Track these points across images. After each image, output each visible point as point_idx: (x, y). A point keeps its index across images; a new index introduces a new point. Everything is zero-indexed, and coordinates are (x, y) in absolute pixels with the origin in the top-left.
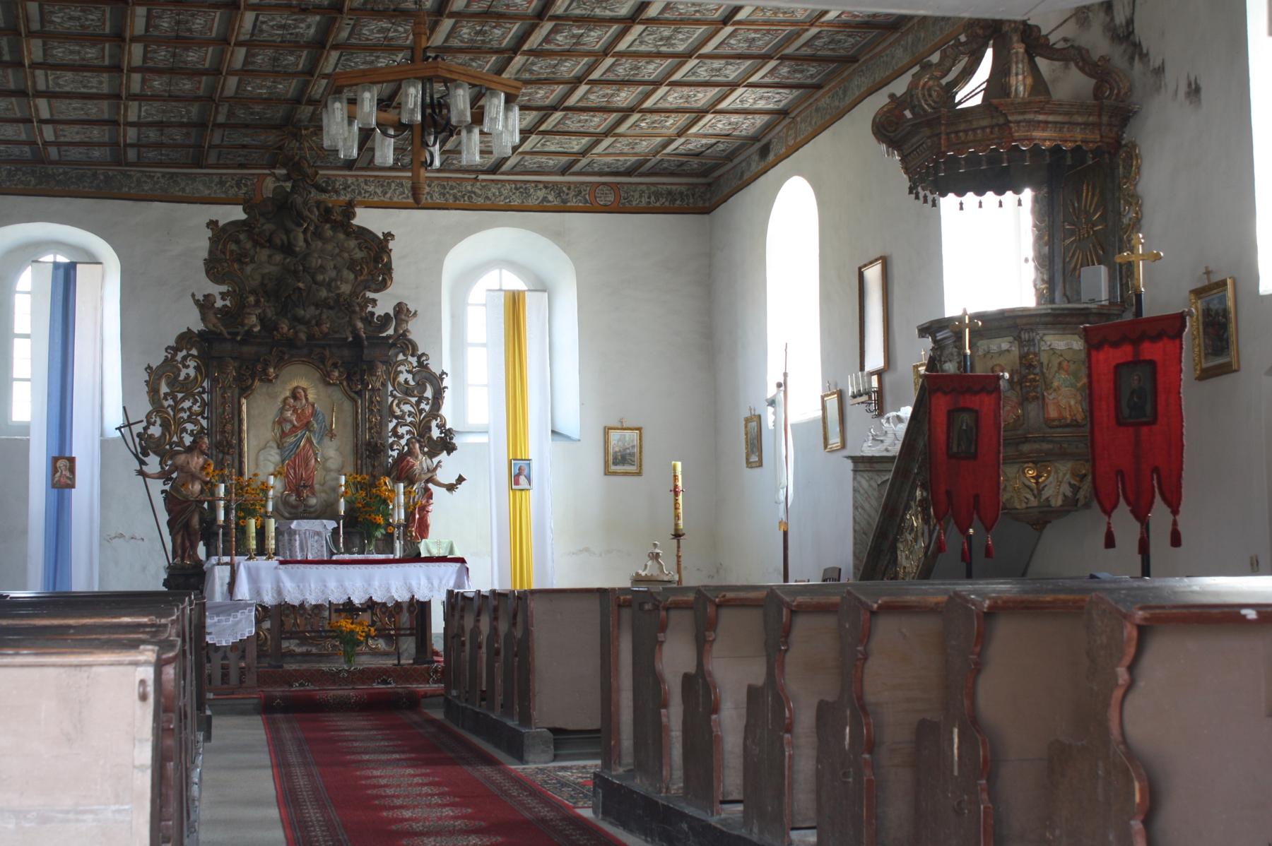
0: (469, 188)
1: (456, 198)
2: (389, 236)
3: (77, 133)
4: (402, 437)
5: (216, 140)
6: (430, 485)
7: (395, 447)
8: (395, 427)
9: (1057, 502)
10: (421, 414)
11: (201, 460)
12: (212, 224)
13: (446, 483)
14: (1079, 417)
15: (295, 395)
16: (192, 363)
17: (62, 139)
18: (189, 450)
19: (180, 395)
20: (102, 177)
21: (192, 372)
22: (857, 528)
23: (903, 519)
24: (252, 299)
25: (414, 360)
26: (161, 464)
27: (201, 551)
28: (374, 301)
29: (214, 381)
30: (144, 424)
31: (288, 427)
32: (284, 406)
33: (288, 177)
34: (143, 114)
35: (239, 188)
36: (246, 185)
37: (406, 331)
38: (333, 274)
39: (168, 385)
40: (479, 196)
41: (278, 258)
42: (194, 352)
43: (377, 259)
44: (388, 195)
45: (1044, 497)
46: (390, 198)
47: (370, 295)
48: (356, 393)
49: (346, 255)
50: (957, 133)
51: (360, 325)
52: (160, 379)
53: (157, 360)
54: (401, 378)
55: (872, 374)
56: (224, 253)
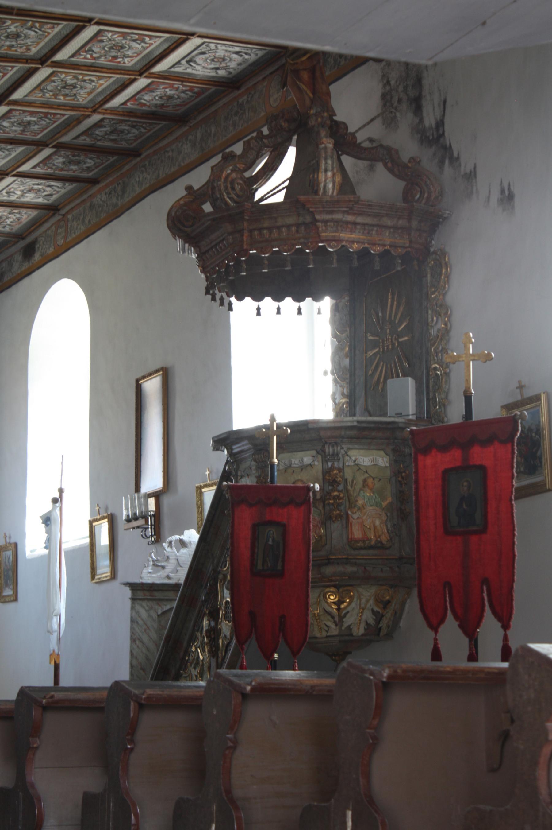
9: (359, 631)
14: (384, 539)
22: (135, 662)
23: (187, 652)
45: (345, 625)
50: (260, 230)
55: (149, 495)
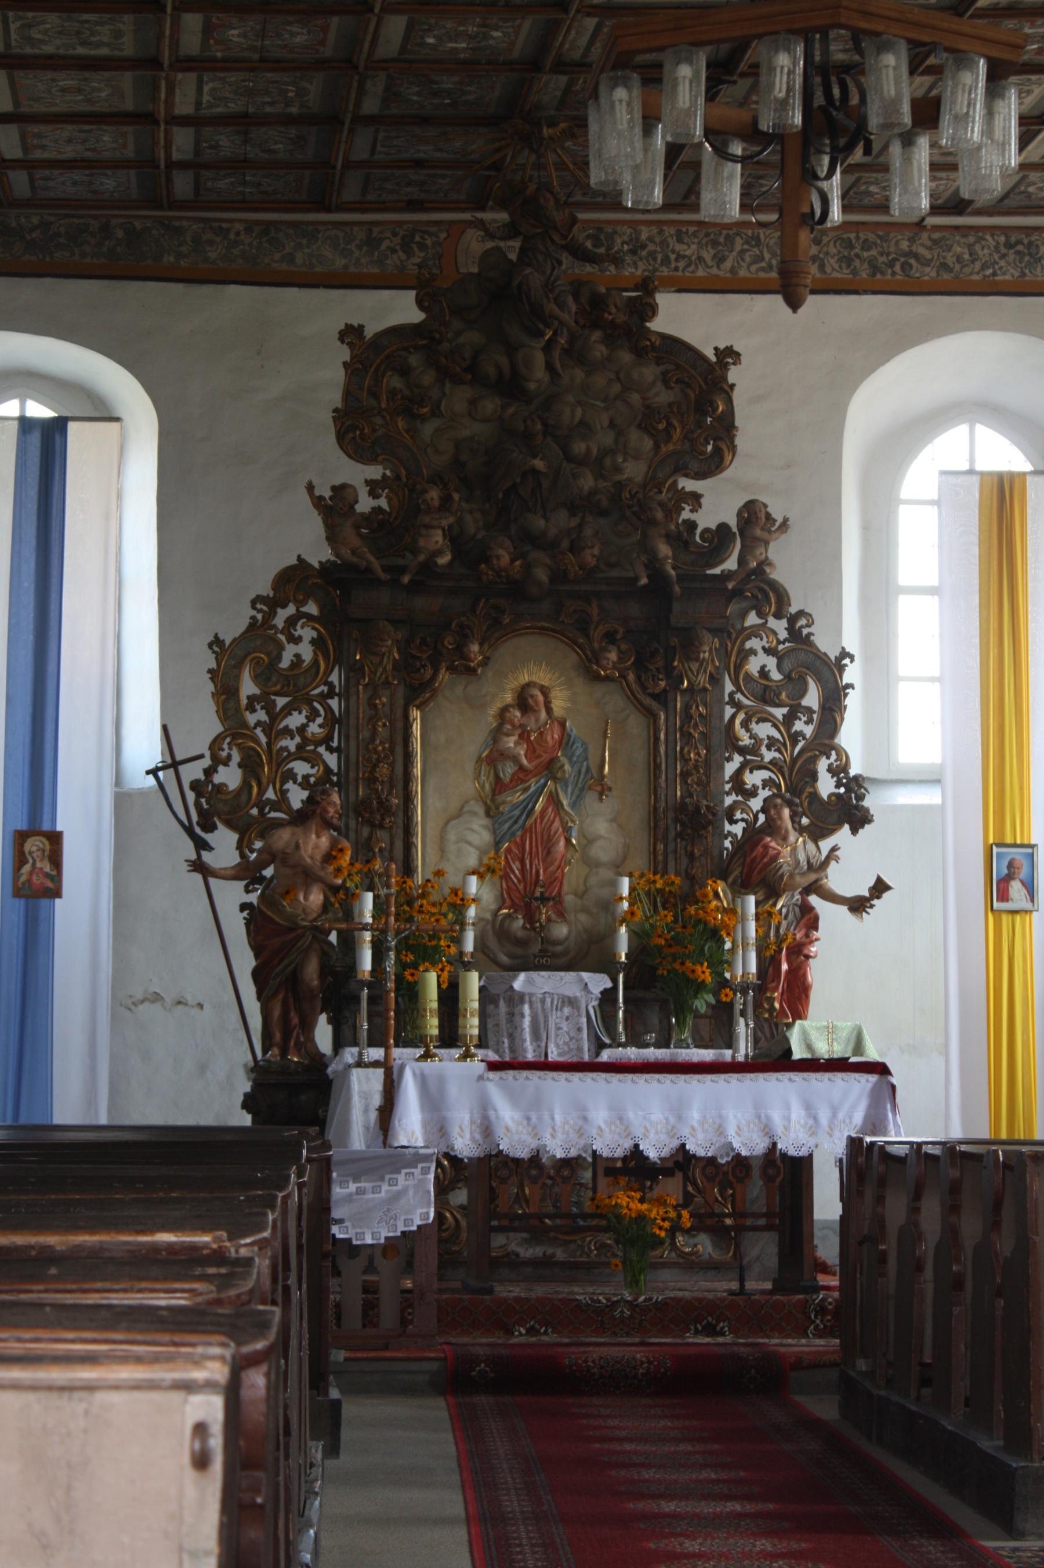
0: (904, 245)
1: (875, 269)
2: (728, 355)
3: (69, 141)
4: (753, 793)
5: (360, 150)
6: (814, 900)
7: (738, 815)
8: (739, 772)
10: (794, 743)
11: (324, 841)
12: (351, 334)
13: (849, 893)
15: (523, 702)
16: (307, 633)
17: (38, 154)
18: (301, 818)
19: (281, 702)
20: (120, 234)
21: (306, 651)
24: (434, 495)
25: (780, 627)
26: (240, 847)
27: (323, 1034)
28: (695, 499)
29: (354, 672)
30: (206, 762)
31: (508, 770)
32: (500, 726)
33: (511, 231)
34: (206, 98)
35: (409, 253)
36: (422, 246)
37: (766, 562)
38: (608, 439)
39: (256, 678)
40: (926, 263)
41: (490, 405)
42: (312, 608)
43: (703, 406)
44: (728, 264)
46: (733, 270)
47: (687, 484)
48: (655, 697)
49: (635, 398)
51: (664, 550)
52: (239, 666)
53: (232, 629)
54: (753, 666)
56: (374, 394)
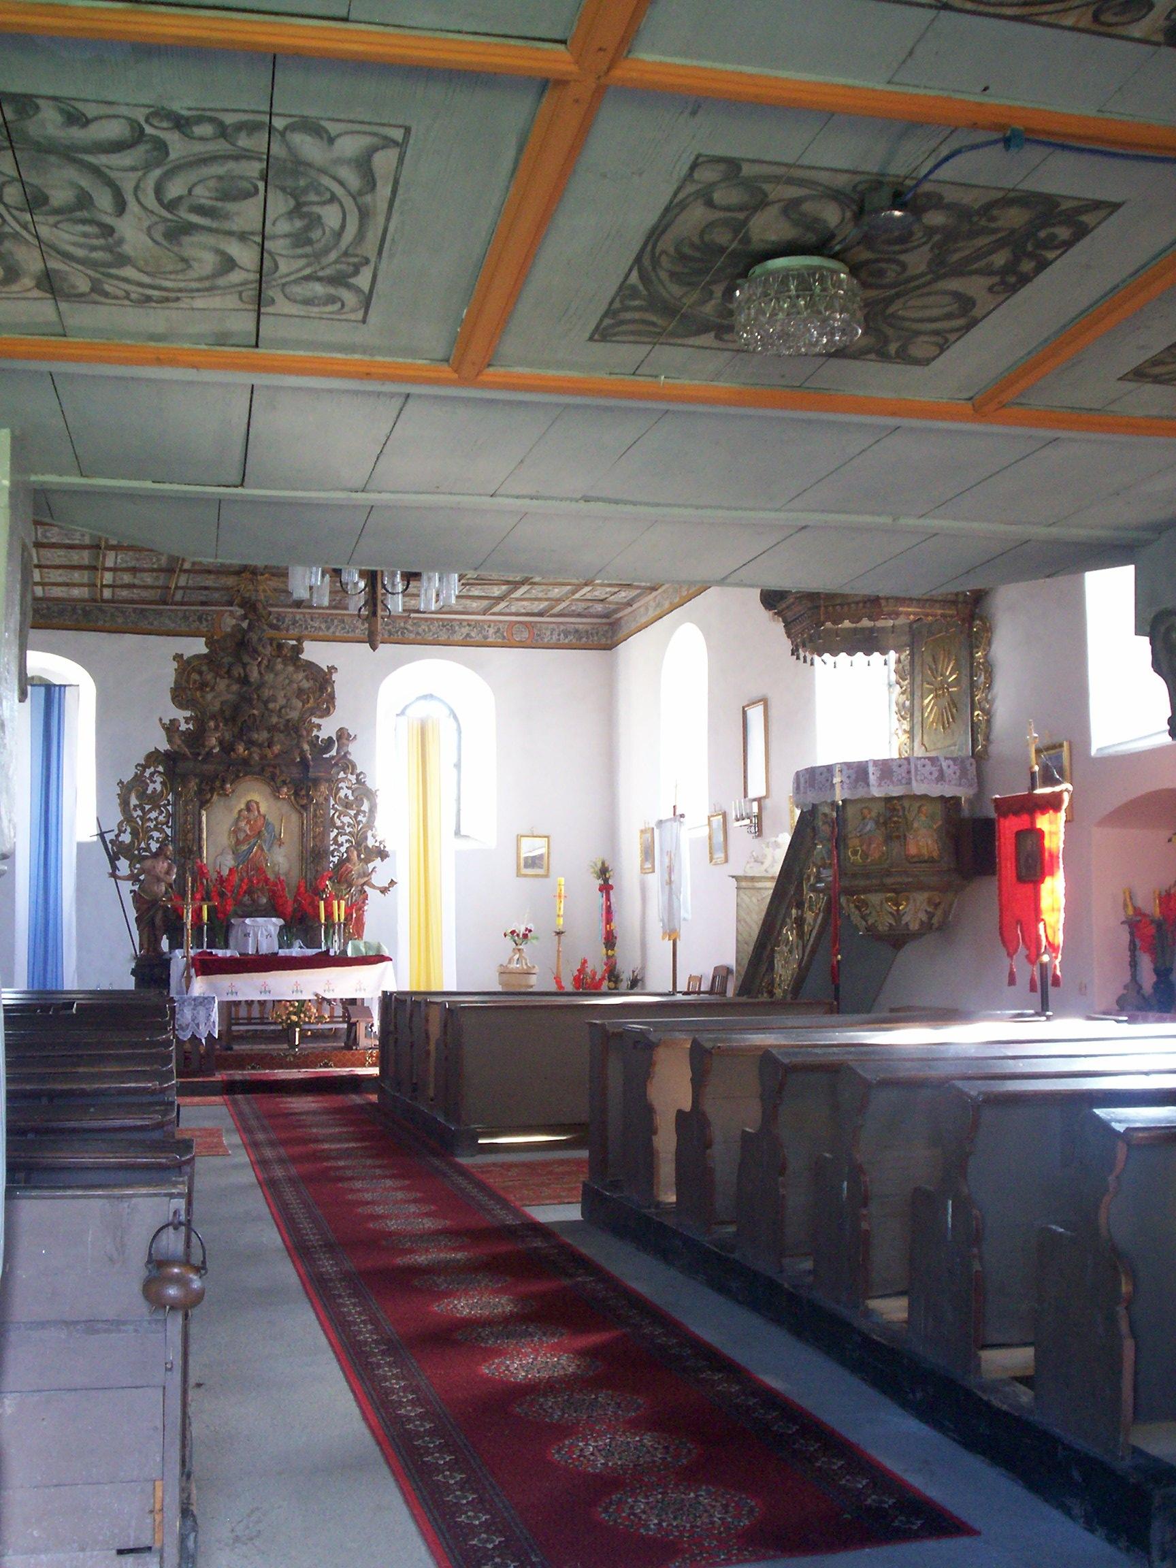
0: (402, 624)
1: (390, 633)
2: (332, 669)
3: (60, 575)
4: (342, 845)
5: (182, 583)
6: (366, 888)
7: (336, 854)
8: (336, 836)
9: (914, 926)
10: (358, 825)
11: (166, 865)
12: (178, 657)
13: (380, 886)
14: (935, 854)
15: (248, 808)
16: (159, 779)
17: (47, 580)
18: (155, 855)
19: (147, 807)
20: (80, 612)
21: (159, 787)
22: (740, 938)
23: (780, 932)
24: (212, 724)
25: (353, 778)
26: (130, 866)
27: (165, 944)
28: (319, 727)
29: (178, 795)
30: (116, 832)
31: (242, 836)
32: (239, 817)
33: (245, 617)
34: (119, 560)
35: (201, 622)
36: (207, 621)
37: (347, 753)
38: (282, 701)
39: (137, 797)
40: (411, 632)
41: (235, 687)
42: (161, 769)
43: (322, 689)
44: (331, 630)
45: (903, 922)
46: (334, 633)
47: (315, 720)
48: (302, 806)
49: (295, 686)
50: (834, 606)
51: (306, 747)
52: (130, 793)
53: (128, 776)
54: (342, 794)
55: (754, 800)
56: (188, 682)
